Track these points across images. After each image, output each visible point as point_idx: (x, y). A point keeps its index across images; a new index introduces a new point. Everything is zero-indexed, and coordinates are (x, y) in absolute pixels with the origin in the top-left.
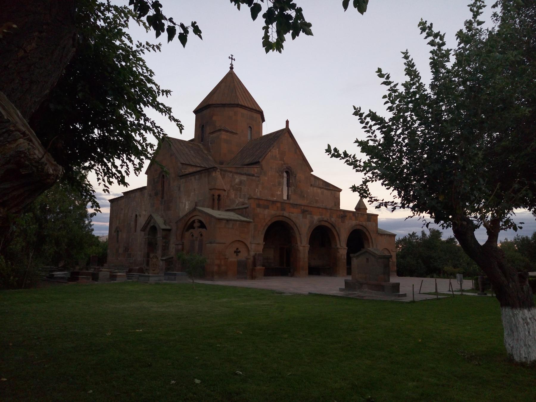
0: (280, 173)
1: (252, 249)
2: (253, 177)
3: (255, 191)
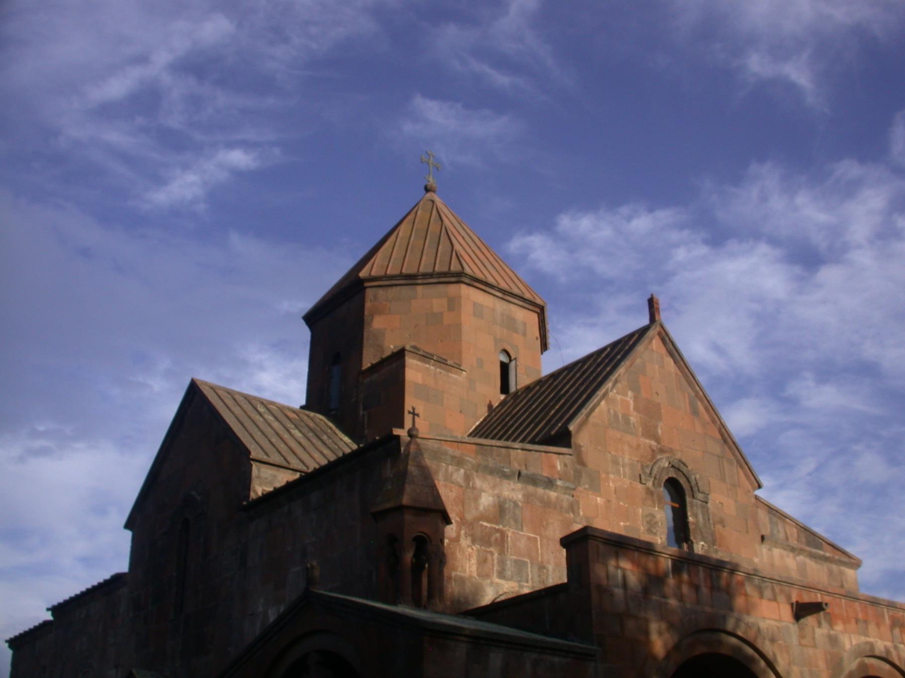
2: (547, 491)
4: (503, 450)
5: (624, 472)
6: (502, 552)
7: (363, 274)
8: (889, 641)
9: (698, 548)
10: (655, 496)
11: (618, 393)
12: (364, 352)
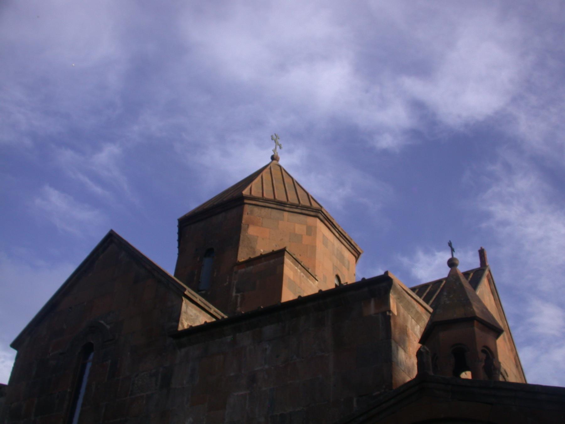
7: (246, 192)
12: (240, 250)
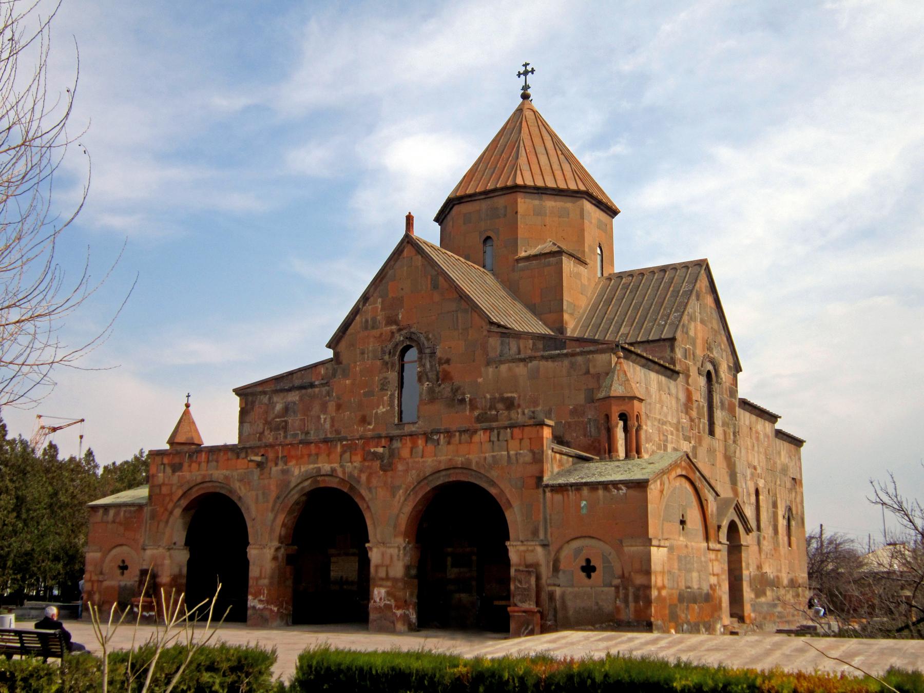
0: (386, 357)
1: (144, 560)
2: (314, 389)
3: (319, 417)
4: (290, 376)
5: (368, 357)
6: (285, 432)
8: (337, 463)
9: (423, 389)
10: (389, 365)
11: (369, 305)
